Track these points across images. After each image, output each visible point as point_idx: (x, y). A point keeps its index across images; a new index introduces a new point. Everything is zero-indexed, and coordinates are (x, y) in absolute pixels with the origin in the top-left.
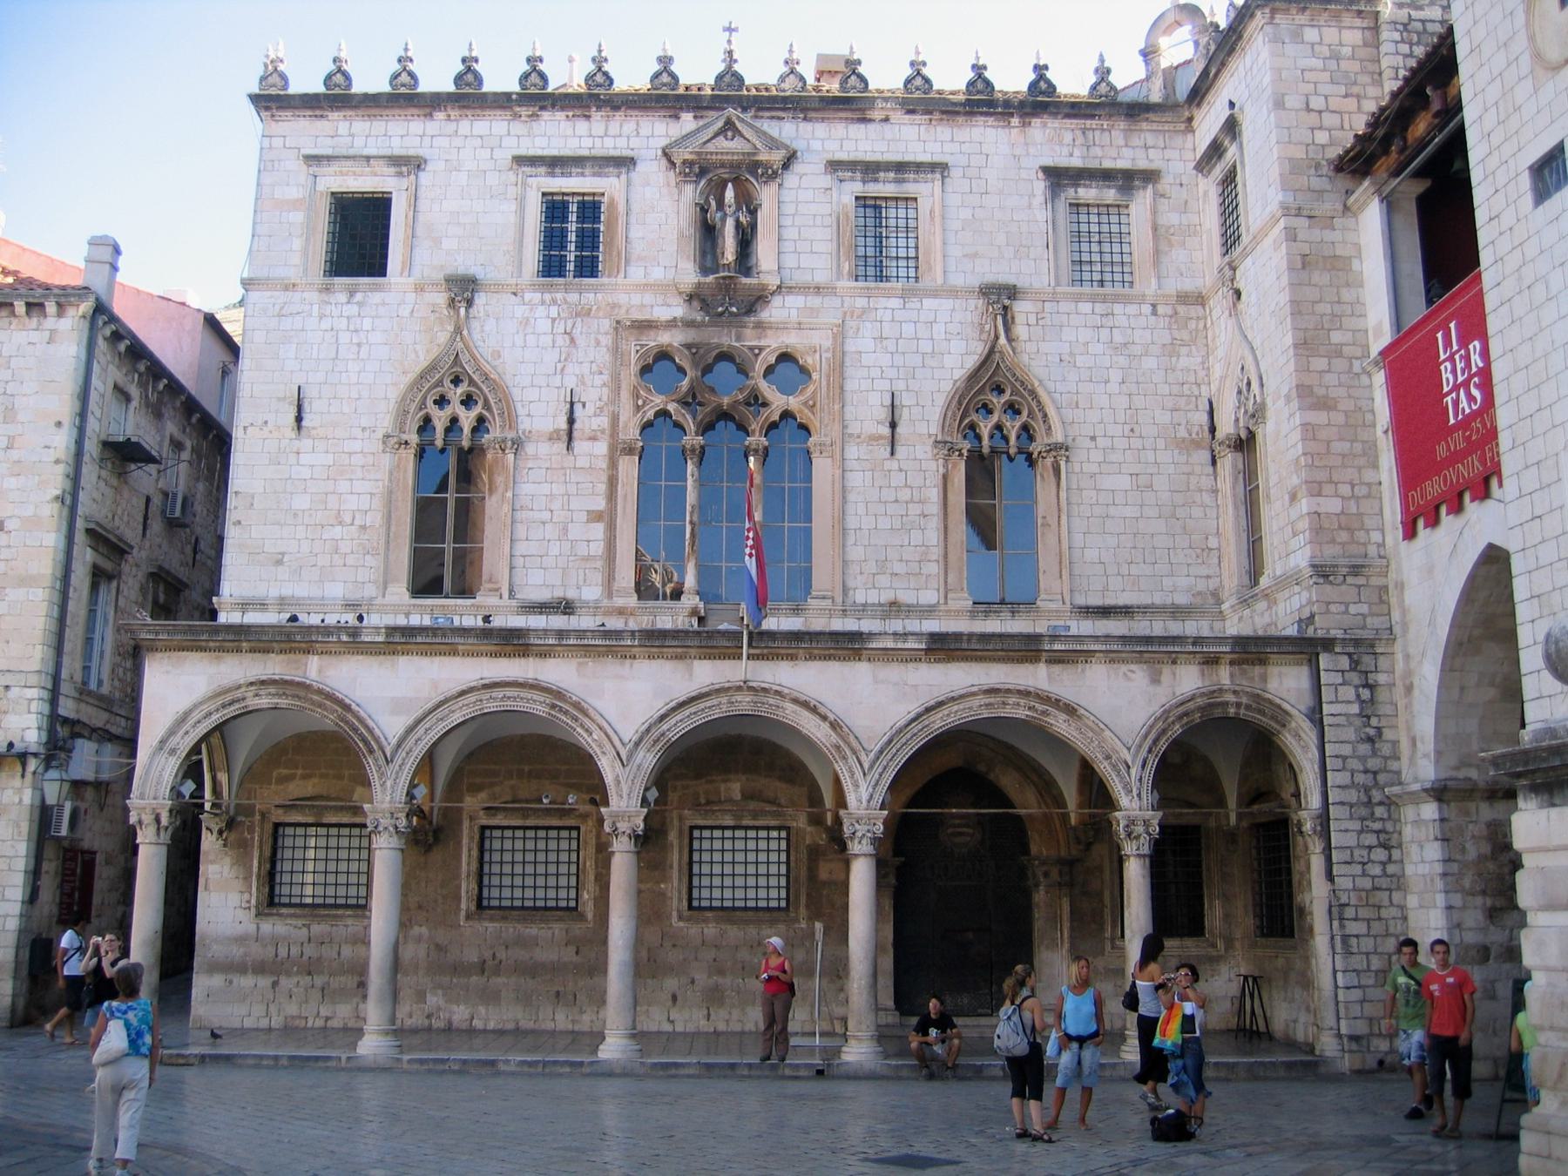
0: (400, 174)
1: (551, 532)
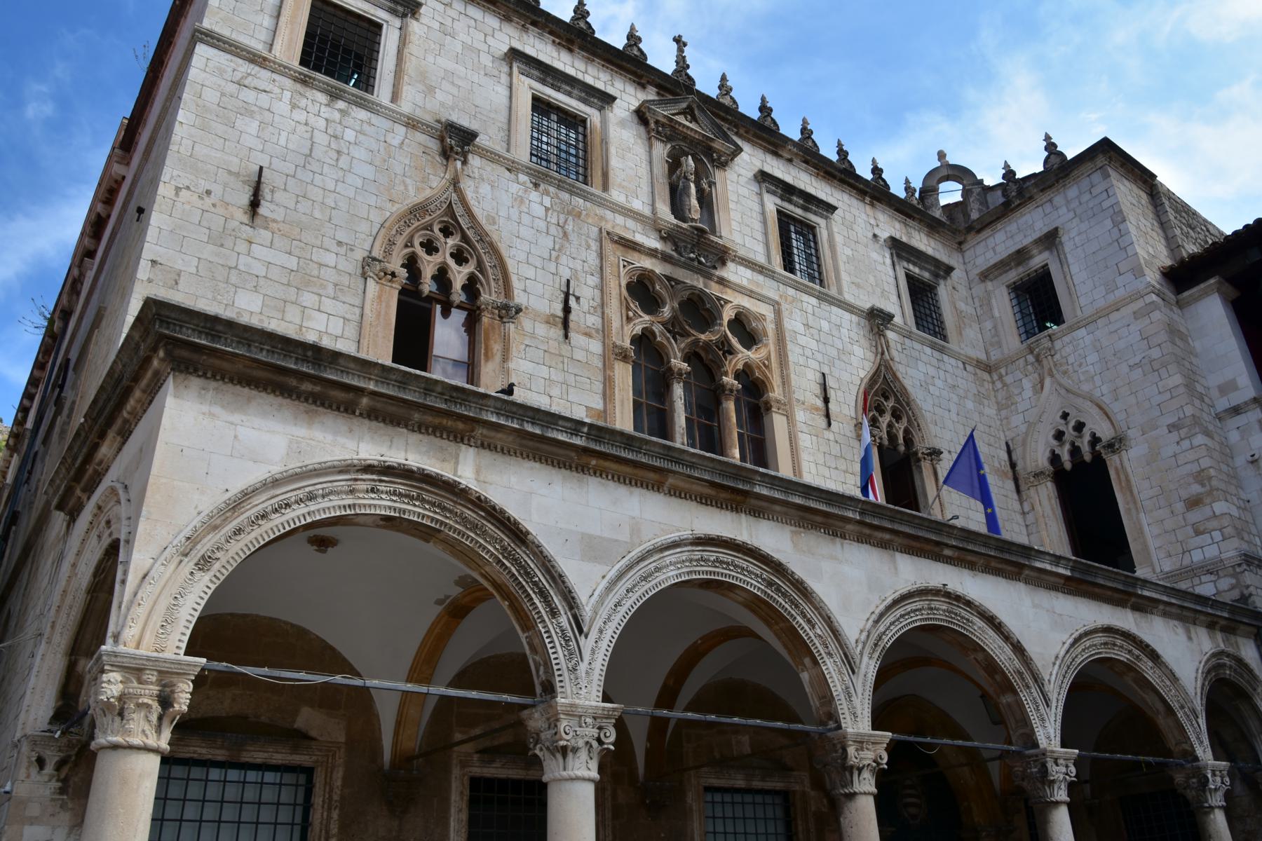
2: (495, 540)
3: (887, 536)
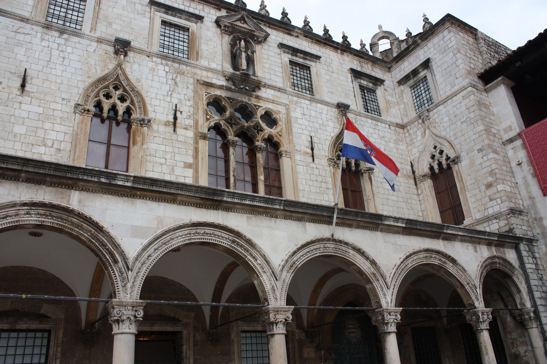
2: (88, 231)
3: (301, 215)
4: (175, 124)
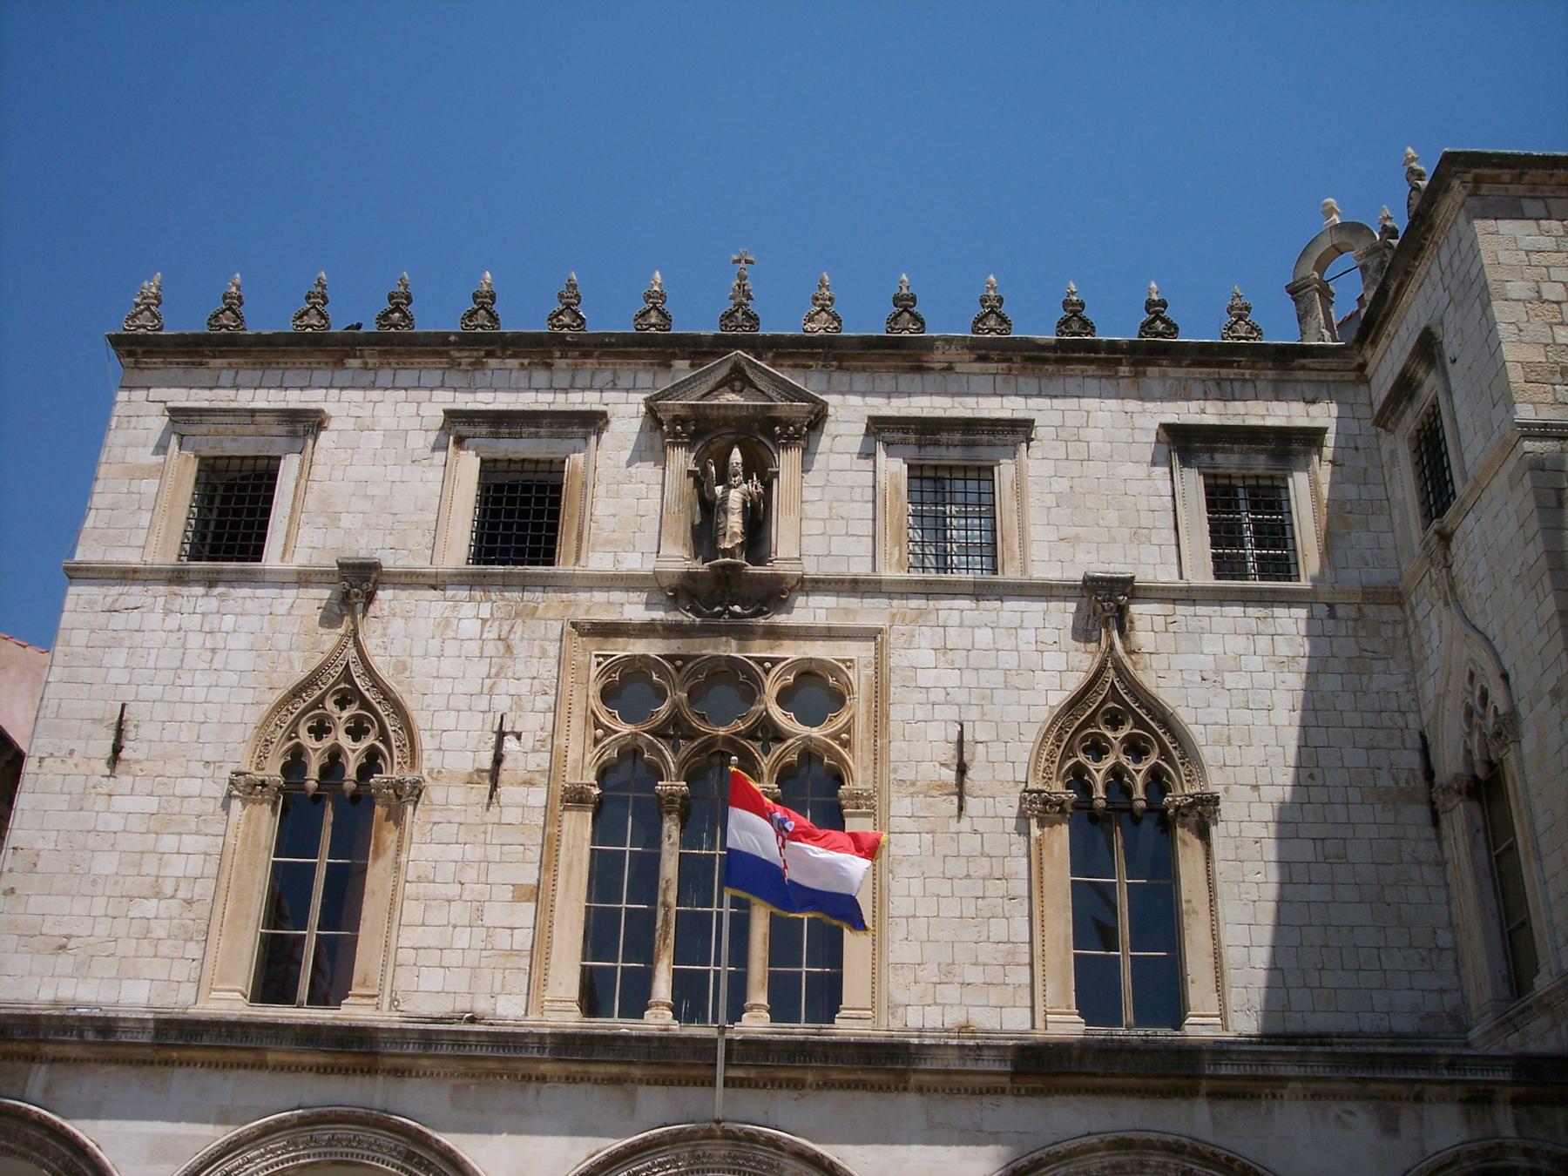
0: (293, 434)
1: (459, 912)
4: (494, 775)
